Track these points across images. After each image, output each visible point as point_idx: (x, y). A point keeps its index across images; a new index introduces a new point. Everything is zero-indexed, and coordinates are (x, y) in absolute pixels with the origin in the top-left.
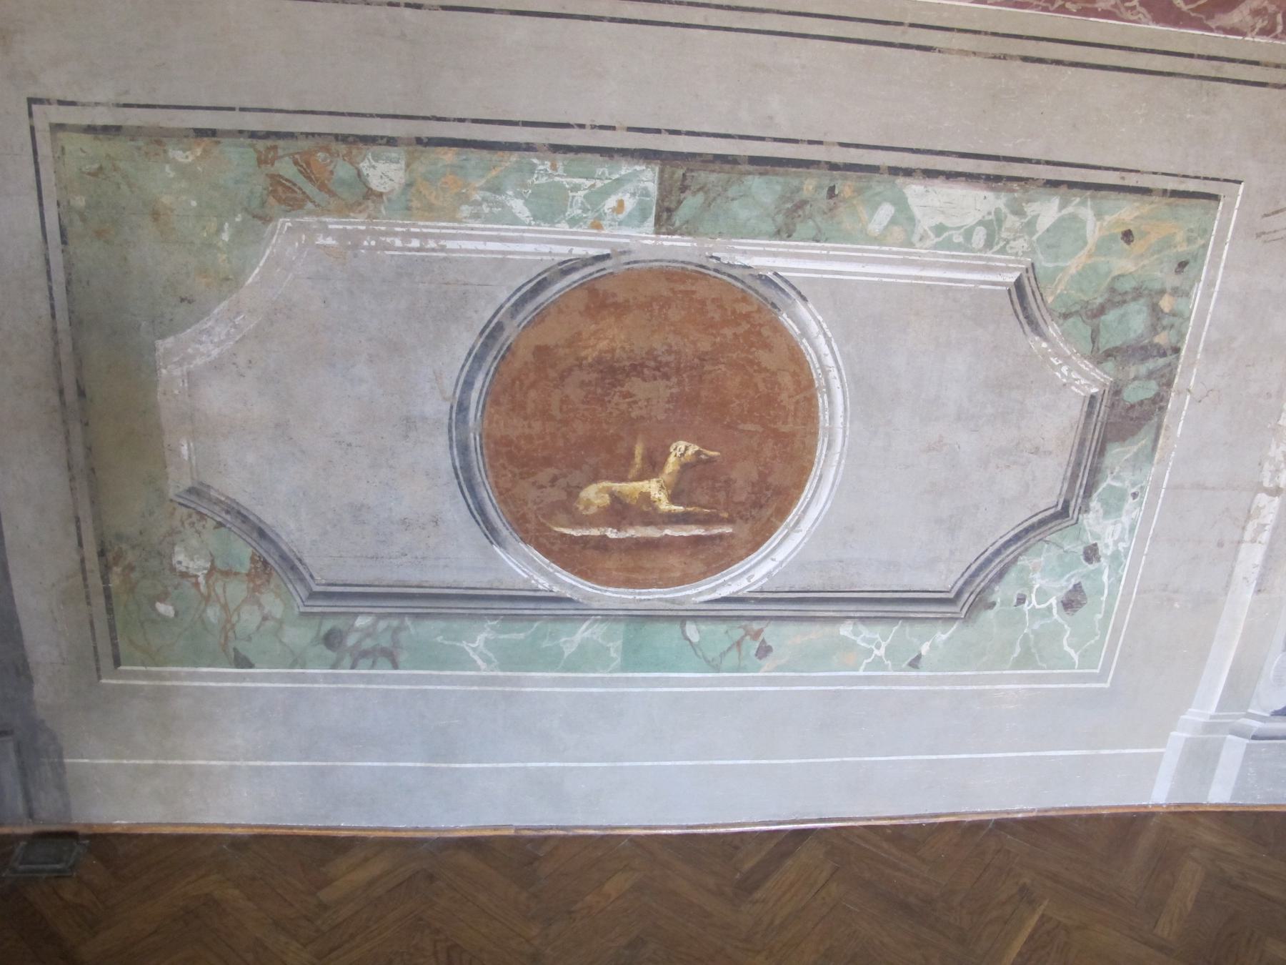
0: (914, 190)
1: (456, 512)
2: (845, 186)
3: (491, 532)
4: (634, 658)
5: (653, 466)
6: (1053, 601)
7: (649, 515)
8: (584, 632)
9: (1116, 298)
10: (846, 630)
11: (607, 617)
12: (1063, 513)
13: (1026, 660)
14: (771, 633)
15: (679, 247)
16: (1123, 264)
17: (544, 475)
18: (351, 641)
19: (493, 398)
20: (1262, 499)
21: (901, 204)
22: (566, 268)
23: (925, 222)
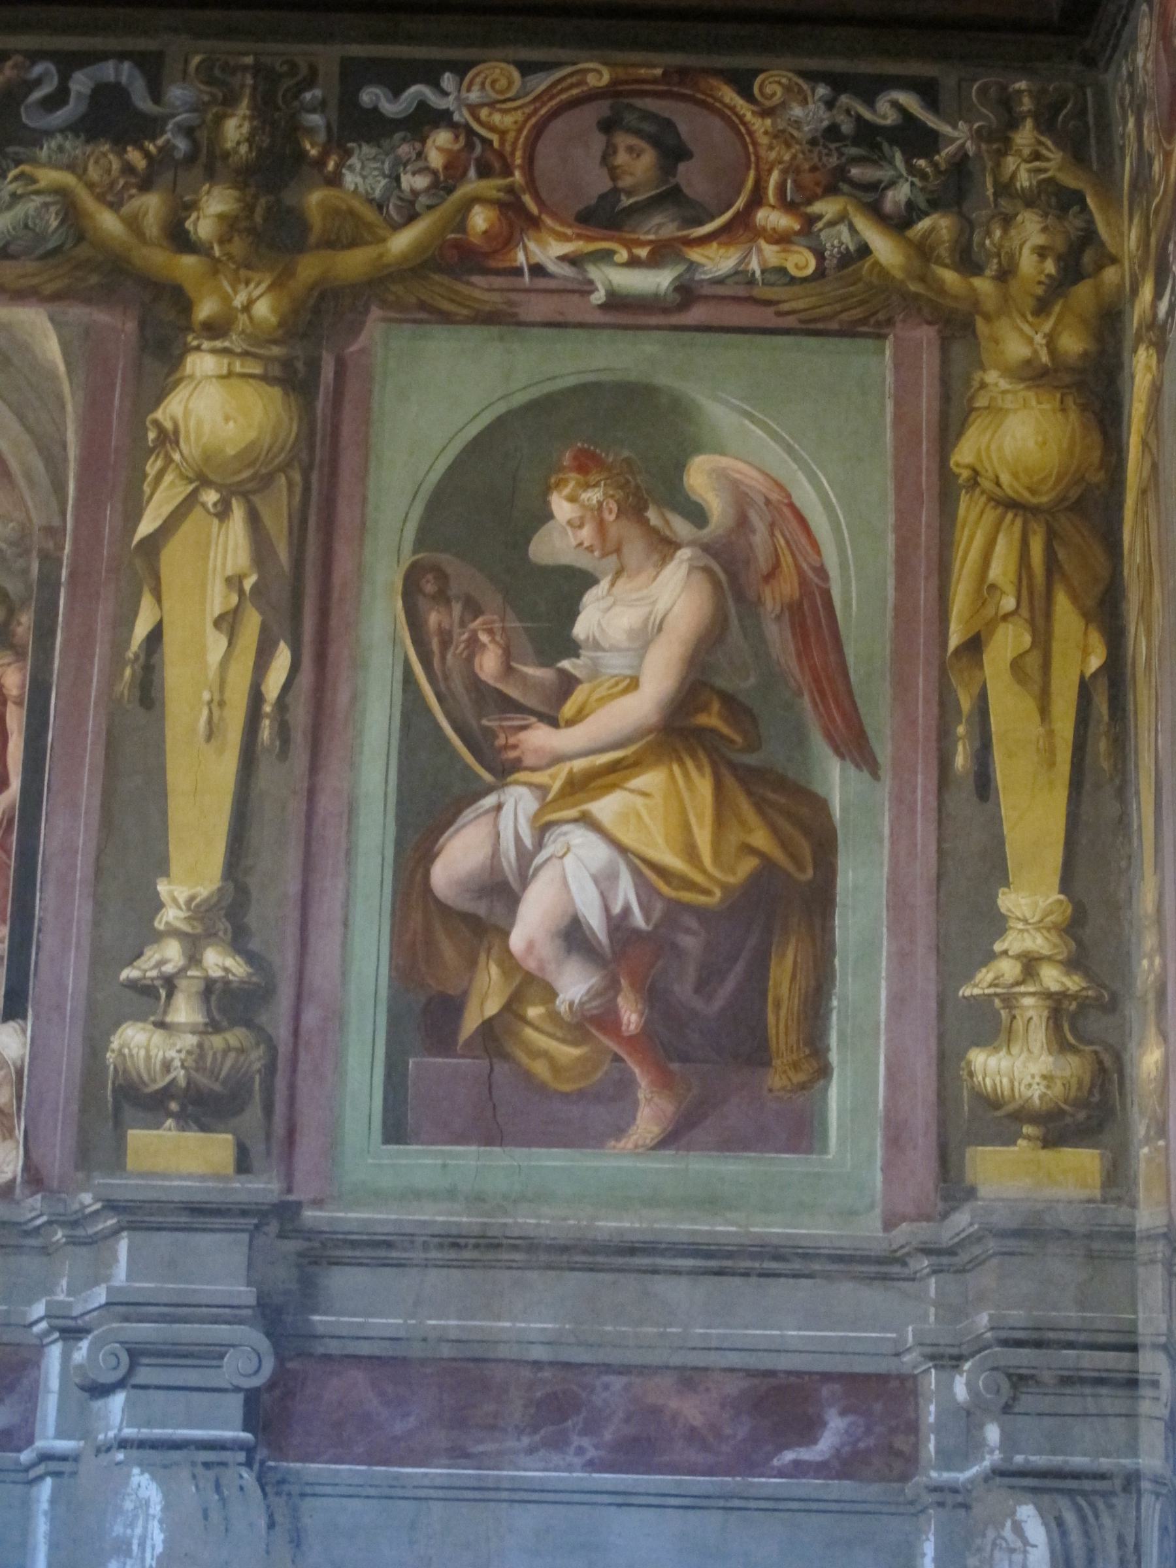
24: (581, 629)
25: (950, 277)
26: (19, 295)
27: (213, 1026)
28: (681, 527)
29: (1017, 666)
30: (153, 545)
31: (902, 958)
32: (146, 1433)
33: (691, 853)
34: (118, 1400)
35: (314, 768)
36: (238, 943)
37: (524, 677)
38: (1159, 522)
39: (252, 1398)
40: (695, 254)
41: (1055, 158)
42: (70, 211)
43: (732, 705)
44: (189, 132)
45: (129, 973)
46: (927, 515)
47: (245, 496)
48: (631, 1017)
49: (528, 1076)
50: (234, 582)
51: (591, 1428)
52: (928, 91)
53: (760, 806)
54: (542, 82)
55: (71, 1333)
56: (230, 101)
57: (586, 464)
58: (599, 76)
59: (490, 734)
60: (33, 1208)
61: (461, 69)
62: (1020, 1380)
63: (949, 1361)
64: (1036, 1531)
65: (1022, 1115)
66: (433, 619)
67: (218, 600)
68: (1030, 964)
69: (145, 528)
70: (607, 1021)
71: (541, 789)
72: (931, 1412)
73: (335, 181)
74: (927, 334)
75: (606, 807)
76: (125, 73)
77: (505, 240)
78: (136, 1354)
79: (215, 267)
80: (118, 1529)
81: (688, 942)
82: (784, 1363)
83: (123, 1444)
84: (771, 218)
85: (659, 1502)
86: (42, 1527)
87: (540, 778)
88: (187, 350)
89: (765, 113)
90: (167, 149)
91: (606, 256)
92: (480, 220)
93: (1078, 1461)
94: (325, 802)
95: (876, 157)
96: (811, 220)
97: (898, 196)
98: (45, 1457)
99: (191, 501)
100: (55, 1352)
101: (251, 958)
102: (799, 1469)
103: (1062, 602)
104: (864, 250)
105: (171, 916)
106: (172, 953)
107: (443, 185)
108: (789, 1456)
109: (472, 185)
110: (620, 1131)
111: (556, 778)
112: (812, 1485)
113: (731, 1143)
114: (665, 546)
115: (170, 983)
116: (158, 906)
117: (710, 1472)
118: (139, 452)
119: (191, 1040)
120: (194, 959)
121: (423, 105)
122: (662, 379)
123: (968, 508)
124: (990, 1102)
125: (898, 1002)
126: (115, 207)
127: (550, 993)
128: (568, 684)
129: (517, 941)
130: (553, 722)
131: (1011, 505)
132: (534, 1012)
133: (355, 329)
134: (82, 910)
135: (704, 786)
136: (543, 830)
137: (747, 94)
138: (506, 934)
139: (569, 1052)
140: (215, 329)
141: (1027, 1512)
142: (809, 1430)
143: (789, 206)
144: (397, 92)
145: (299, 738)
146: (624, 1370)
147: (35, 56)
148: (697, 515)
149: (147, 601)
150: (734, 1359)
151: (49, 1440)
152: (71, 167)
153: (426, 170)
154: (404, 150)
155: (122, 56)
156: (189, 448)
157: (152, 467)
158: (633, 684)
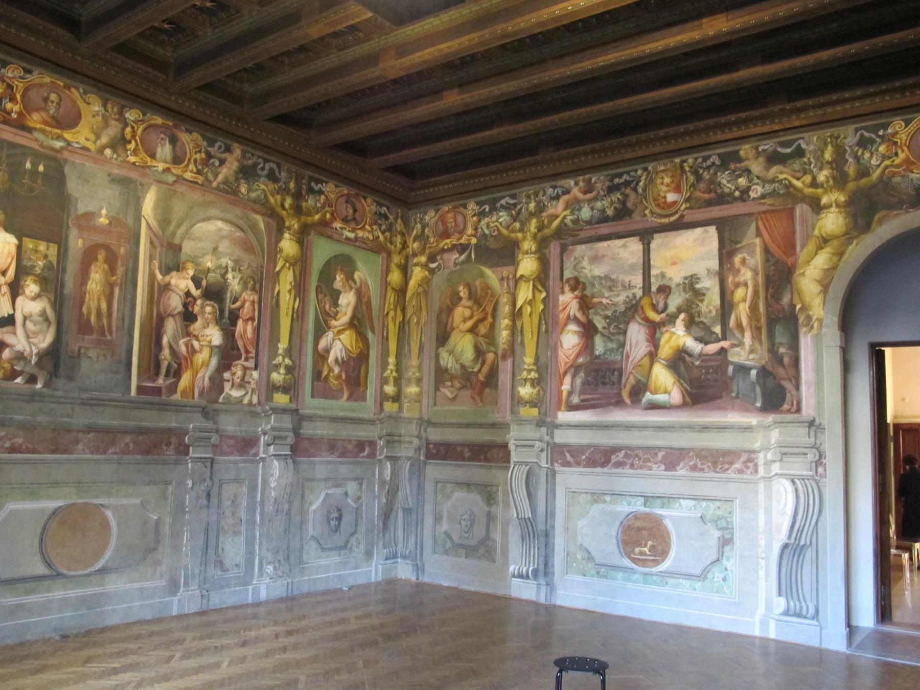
0: (682, 501)
1: (617, 551)
2: (671, 500)
3: (622, 556)
4: (645, 582)
5: (646, 545)
6: (720, 579)
7: (646, 555)
8: (636, 576)
9: (719, 519)
10: (681, 580)
11: (640, 573)
12: (718, 560)
13: (717, 592)
14: (668, 580)
15: (647, 510)
16: (719, 513)
17: (630, 546)
18: (601, 573)
19: (622, 533)
20: (760, 560)
21: (680, 503)
22: (632, 513)
23: (684, 506)
24: (340, 302)
25: (389, 245)
26: (258, 213)
27: (286, 374)
28: (353, 285)
29: (392, 318)
30: (278, 273)
31: (377, 369)
32: (277, 453)
33: (352, 347)
34: (272, 447)
35: (302, 325)
36: (290, 358)
37: (332, 311)
38: (427, 303)
39: (292, 446)
40: (357, 231)
41: (403, 226)
42: (266, 196)
43: (359, 321)
44: (285, 183)
45: (274, 362)
46: (384, 288)
47: (293, 266)
48: (344, 377)
49: (330, 387)
50: (291, 283)
51: (337, 450)
52: (388, 208)
53: (361, 339)
54: (338, 190)
55: (265, 434)
56: (291, 178)
57: (342, 270)
58: (346, 192)
59: (327, 321)
60: (259, 409)
61: (326, 183)
62: (388, 442)
63: (380, 438)
64: (389, 466)
65: (390, 397)
66: (320, 297)
67: (288, 287)
68: (392, 371)
69: (278, 269)
70: (340, 377)
71: (333, 332)
72: (378, 447)
73: (307, 201)
74: (385, 255)
75: (342, 337)
76: (274, 166)
77: (332, 222)
78: (275, 438)
79: (288, 214)
80: (272, 472)
81: (352, 364)
82: (362, 439)
83: (273, 455)
84: (368, 227)
85: (345, 463)
86: (260, 472)
87: (333, 330)
88: (284, 232)
89: (368, 206)
90: (281, 186)
91: (345, 229)
92: (328, 216)
93: (394, 455)
94: (303, 332)
95: (381, 219)
96: (372, 229)
97: (383, 227)
98: (261, 458)
99: (284, 265)
100: (262, 437)
101: (293, 361)
102: (363, 457)
103: (398, 308)
104: (379, 237)
105: (280, 351)
106: (280, 359)
107: (323, 207)
108: (362, 455)
109: (327, 208)
110: (342, 397)
111: (335, 330)
112: (363, 460)
113: (356, 400)
114: (351, 288)
115: (280, 364)
116: (278, 348)
117: (352, 457)
118: (277, 253)
119: (283, 376)
120: (284, 360)
121: (320, 189)
122: (352, 255)
123: (389, 288)
124: (386, 395)
125: (376, 376)
126: (273, 196)
127: (333, 371)
128: (337, 312)
129: (329, 361)
130: (335, 319)
131: (394, 289)
132: (331, 374)
133: (309, 234)
134: (267, 349)
135: (354, 335)
136: (334, 340)
137: (365, 201)
138: (328, 359)
139: (336, 382)
140: (289, 228)
141: (388, 463)
142: (363, 450)
143: (370, 226)
144: (317, 185)
145: (300, 319)
146: (341, 440)
147: (260, 157)
148: (355, 283)
149: (277, 285)
150: (355, 438)
151: (262, 455)
152: (266, 185)
153: (320, 203)
154: (318, 198)
155: (274, 162)
156: (284, 254)
157: (279, 256)
158: (346, 314)
